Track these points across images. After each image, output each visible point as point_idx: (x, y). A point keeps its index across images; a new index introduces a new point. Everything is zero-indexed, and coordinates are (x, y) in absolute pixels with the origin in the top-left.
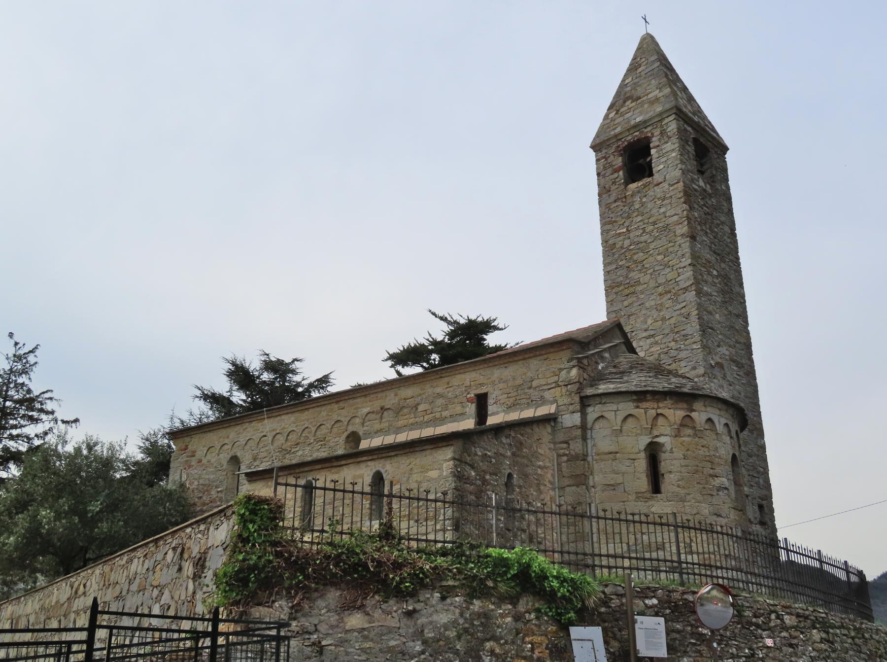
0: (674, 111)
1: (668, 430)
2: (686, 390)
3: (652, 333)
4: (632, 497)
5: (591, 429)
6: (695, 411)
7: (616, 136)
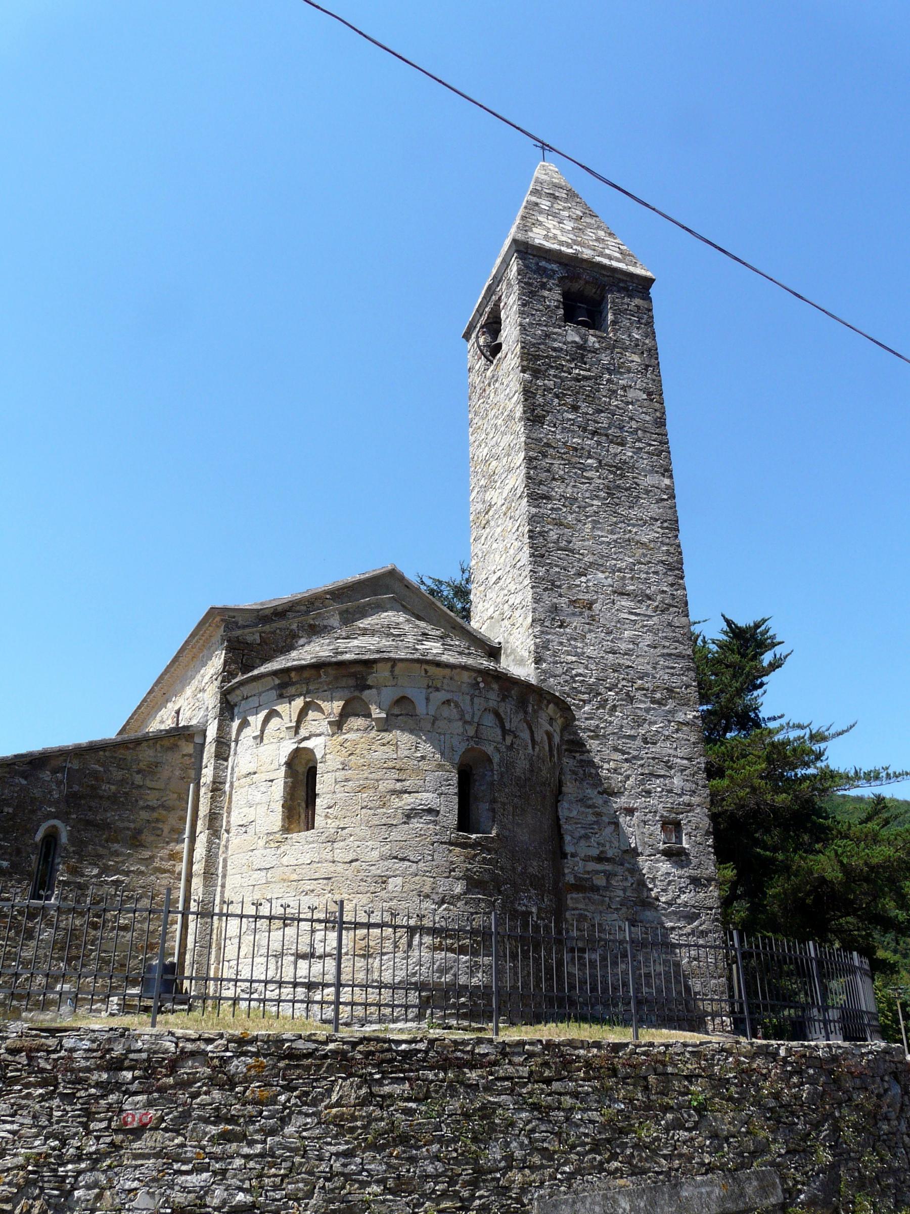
0: (514, 248)
1: (324, 727)
2: (347, 657)
3: (498, 574)
4: (261, 843)
5: (237, 741)
6: (370, 687)
7: (477, 310)
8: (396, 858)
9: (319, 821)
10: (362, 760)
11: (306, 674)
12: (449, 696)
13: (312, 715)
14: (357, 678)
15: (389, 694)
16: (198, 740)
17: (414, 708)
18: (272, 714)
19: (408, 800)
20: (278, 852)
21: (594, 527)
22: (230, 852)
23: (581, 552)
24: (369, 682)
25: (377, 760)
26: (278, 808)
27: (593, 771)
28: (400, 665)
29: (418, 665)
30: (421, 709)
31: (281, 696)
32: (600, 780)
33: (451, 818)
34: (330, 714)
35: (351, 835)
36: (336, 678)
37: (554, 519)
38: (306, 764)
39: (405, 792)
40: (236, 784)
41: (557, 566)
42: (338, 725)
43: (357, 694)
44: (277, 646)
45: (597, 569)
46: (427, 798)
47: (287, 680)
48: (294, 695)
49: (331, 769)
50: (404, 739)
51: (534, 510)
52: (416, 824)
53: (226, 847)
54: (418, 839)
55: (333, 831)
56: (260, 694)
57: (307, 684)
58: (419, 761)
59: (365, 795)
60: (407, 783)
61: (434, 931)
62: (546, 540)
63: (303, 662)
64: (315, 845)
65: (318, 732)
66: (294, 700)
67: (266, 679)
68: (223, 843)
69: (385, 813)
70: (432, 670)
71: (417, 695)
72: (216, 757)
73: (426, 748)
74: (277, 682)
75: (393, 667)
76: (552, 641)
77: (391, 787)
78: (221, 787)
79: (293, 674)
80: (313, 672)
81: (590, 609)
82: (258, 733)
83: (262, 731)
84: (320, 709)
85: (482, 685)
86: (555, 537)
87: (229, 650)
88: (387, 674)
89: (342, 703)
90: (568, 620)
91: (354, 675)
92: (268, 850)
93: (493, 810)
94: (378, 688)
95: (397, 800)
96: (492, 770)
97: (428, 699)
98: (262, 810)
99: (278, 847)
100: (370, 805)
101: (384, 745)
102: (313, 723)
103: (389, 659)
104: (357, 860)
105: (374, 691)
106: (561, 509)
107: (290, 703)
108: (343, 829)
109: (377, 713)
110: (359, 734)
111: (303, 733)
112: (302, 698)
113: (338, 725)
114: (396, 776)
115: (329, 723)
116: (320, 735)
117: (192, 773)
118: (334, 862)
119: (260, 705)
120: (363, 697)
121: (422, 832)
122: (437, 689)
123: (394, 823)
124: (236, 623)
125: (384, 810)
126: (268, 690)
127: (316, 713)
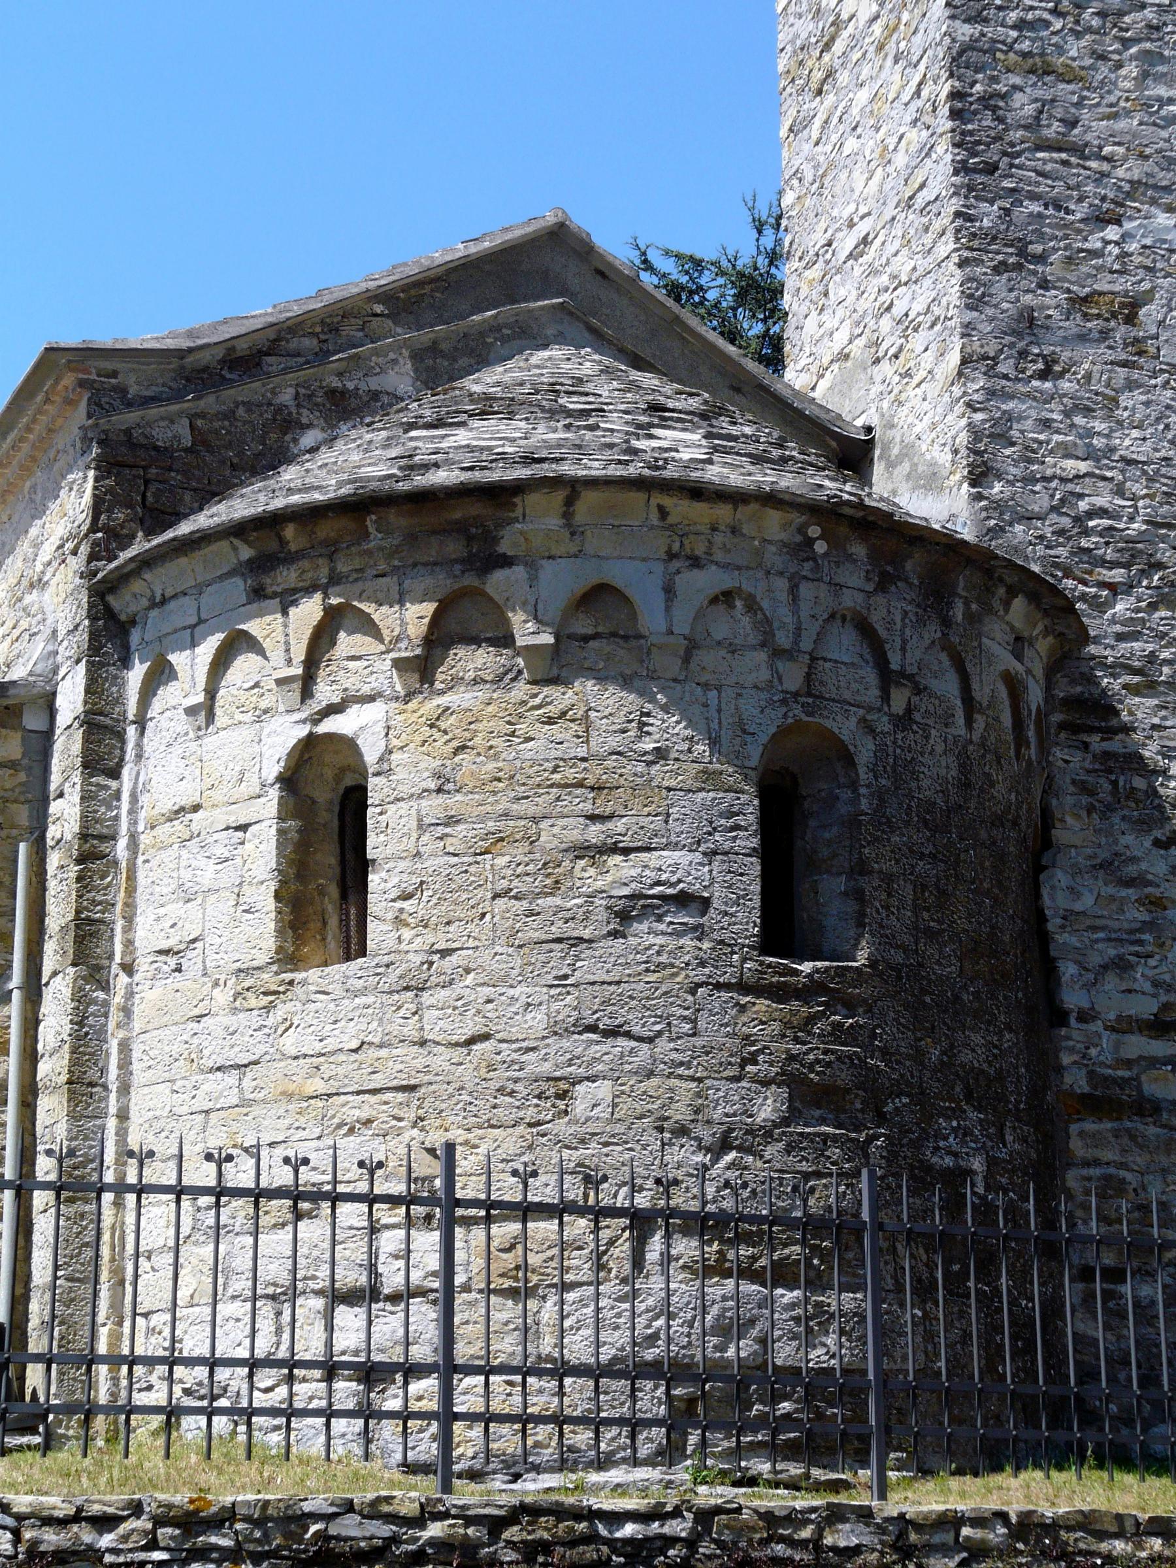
1: (381, 674)
2: (441, 477)
3: (863, 228)
4: (222, 997)
5: (141, 722)
6: (506, 562)
8: (592, 1029)
9: (377, 932)
10: (491, 766)
11: (326, 529)
12: (727, 581)
13: (346, 643)
14: (470, 539)
15: (561, 580)
16: (33, 721)
17: (633, 616)
18: (237, 644)
19: (622, 874)
20: (270, 1022)
21: (1145, 75)
22: (137, 1025)
23: (1107, 150)
24: (505, 547)
25: (534, 762)
26: (264, 899)
27: (1139, 783)
28: (589, 498)
29: (640, 497)
30: (652, 618)
31: (258, 594)
32: (1160, 808)
33: (746, 922)
34: (398, 639)
35: (468, 971)
36: (412, 538)
37: (1025, 55)
38: (338, 779)
39: (615, 849)
40: (145, 840)
41: (1034, 197)
42: (422, 668)
43: (470, 580)
44: (240, 454)
45: (1153, 202)
46: (677, 865)
47: (273, 545)
48: (295, 591)
49: (405, 790)
50: (607, 702)
51: (966, 31)
52: (647, 935)
53: (127, 1011)
54: (652, 977)
55: (417, 959)
56: (200, 589)
57: (331, 557)
58: (649, 764)
59: (501, 861)
60: (619, 825)
61: (701, 1224)
62: (1001, 120)
63: (317, 496)
64: (370, 1000)
65: (366, 690)
66: (295, 603)
67: (214, 547)
68: (118, 1000)
69: (560, 909)
70: (681, 508)
71: (638, 579)
72: (85, 765)
73: (669, 728)
74: (246, 553)
75: (570, 502)
76: (1020, 418)
77: (575, 836)
78: (104, 847)
79: (289, 531)
80: (345, 523)
81: (1131, 320)
82: (200, 698)
83: (211, 693)
84: (369, 627)
85: (820, 547)
86: (1030, 110)
87: (106, 467)
88: (554, 522)
89: (429, 608)
90: (1065, 355)
91: (460, 529)
92: (242, 1015)
93: (859, 896)
94: (532, 565)
95: (592, 871)
96: (854, 785)
97: (669, 591)
98: (221, 908)
99: (269, 1008)
100: (518, 886)
101: (550, 721)
102: (352, 665)
103: (557, 482)
104: (486, 1037)
105: (518, 572)
106: (1047, 24)
107: (285, 613)
108: (445, 953)
109: (528, 632)
110: (481, 693)
111: (325, 693)
112: (318, 597)
113: (422, 668)
114: (587, 807)
115: (398, 664)
116: (371, 699)
117: (22, 815)
118: (423, 1043)
119: (201, 621)
120: (489, 589)
121: (663, 959)
122: (695, 562)
123: (586, 934)
124: (122, 391)
125: (557, 901)
126: (222, 578)
127: (358, 638)
